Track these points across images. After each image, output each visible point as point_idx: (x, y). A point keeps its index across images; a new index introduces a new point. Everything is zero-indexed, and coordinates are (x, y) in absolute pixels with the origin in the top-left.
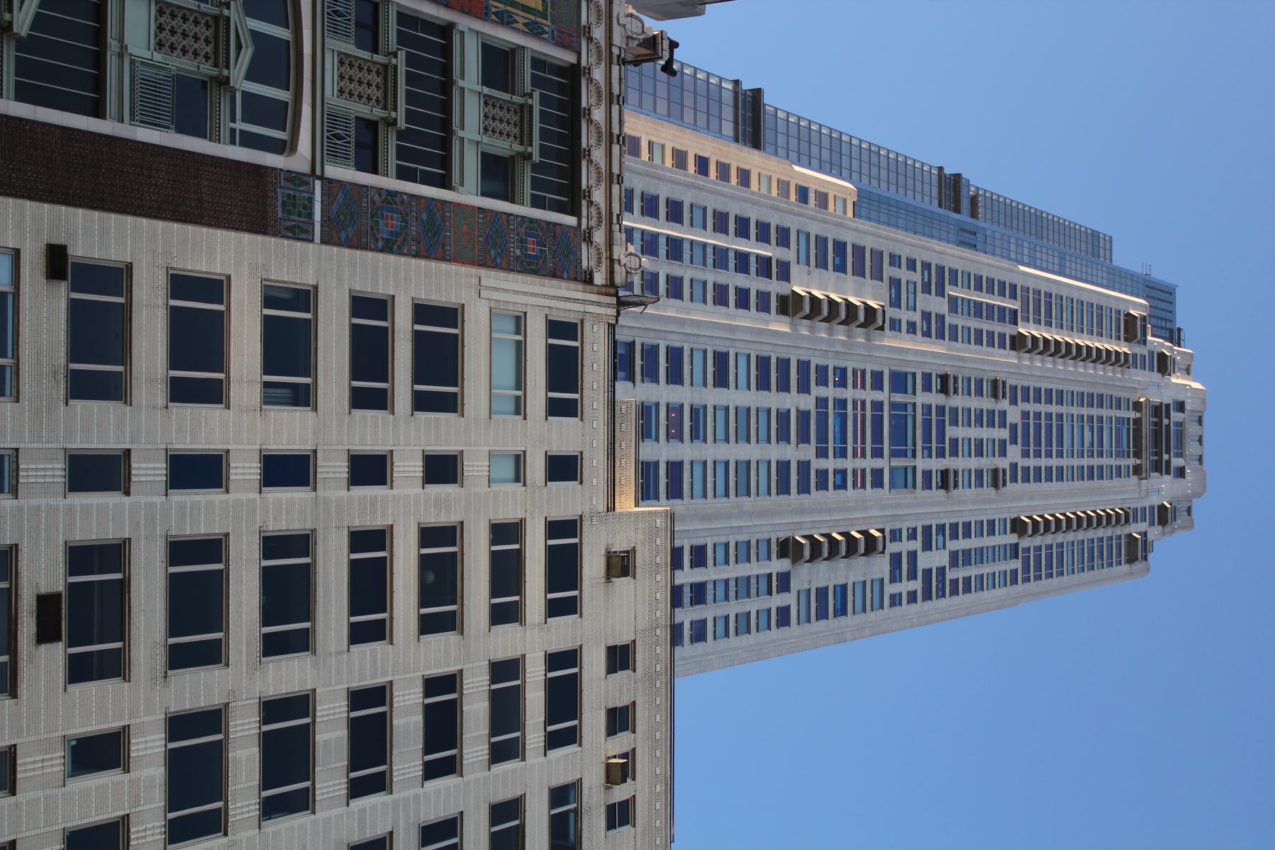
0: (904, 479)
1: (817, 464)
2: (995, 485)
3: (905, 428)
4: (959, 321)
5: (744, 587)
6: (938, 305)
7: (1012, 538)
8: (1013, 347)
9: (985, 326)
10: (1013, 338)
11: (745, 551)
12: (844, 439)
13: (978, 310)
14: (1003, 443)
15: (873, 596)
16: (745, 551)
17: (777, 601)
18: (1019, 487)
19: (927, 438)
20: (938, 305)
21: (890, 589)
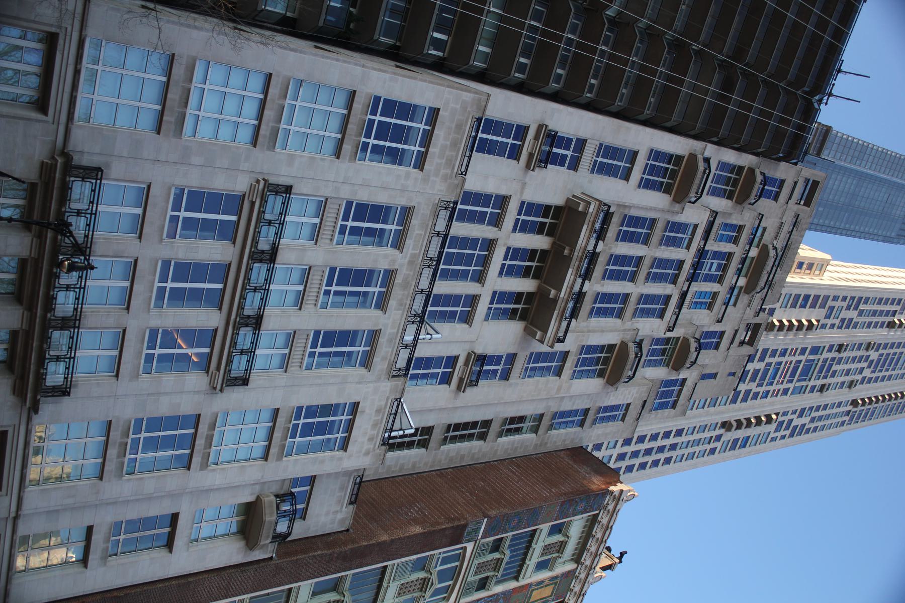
0: (800, 391)
1: (755, 390)
2: (850, 387)
3: (811, 369)
4: (861, 320)
5: (698, 442)
6: (852, 314)
7: (850, 408)
8: (888, 326)
9: (874, 319)
10: (889, 323)
11: (703, 428)
12: (774, 378)
13: (874, 313)
14: (862, 369)
15: (766, 438)
16: (703, 428)
17: (712, 445)
18: (865, 386)
19: (820, 372)
20: (852, 314)
21: (772, 435)
